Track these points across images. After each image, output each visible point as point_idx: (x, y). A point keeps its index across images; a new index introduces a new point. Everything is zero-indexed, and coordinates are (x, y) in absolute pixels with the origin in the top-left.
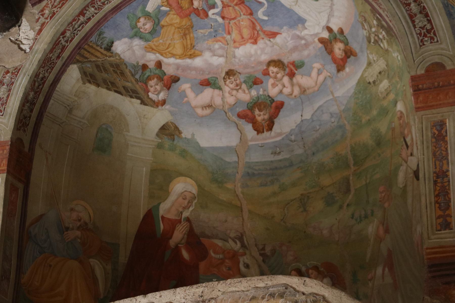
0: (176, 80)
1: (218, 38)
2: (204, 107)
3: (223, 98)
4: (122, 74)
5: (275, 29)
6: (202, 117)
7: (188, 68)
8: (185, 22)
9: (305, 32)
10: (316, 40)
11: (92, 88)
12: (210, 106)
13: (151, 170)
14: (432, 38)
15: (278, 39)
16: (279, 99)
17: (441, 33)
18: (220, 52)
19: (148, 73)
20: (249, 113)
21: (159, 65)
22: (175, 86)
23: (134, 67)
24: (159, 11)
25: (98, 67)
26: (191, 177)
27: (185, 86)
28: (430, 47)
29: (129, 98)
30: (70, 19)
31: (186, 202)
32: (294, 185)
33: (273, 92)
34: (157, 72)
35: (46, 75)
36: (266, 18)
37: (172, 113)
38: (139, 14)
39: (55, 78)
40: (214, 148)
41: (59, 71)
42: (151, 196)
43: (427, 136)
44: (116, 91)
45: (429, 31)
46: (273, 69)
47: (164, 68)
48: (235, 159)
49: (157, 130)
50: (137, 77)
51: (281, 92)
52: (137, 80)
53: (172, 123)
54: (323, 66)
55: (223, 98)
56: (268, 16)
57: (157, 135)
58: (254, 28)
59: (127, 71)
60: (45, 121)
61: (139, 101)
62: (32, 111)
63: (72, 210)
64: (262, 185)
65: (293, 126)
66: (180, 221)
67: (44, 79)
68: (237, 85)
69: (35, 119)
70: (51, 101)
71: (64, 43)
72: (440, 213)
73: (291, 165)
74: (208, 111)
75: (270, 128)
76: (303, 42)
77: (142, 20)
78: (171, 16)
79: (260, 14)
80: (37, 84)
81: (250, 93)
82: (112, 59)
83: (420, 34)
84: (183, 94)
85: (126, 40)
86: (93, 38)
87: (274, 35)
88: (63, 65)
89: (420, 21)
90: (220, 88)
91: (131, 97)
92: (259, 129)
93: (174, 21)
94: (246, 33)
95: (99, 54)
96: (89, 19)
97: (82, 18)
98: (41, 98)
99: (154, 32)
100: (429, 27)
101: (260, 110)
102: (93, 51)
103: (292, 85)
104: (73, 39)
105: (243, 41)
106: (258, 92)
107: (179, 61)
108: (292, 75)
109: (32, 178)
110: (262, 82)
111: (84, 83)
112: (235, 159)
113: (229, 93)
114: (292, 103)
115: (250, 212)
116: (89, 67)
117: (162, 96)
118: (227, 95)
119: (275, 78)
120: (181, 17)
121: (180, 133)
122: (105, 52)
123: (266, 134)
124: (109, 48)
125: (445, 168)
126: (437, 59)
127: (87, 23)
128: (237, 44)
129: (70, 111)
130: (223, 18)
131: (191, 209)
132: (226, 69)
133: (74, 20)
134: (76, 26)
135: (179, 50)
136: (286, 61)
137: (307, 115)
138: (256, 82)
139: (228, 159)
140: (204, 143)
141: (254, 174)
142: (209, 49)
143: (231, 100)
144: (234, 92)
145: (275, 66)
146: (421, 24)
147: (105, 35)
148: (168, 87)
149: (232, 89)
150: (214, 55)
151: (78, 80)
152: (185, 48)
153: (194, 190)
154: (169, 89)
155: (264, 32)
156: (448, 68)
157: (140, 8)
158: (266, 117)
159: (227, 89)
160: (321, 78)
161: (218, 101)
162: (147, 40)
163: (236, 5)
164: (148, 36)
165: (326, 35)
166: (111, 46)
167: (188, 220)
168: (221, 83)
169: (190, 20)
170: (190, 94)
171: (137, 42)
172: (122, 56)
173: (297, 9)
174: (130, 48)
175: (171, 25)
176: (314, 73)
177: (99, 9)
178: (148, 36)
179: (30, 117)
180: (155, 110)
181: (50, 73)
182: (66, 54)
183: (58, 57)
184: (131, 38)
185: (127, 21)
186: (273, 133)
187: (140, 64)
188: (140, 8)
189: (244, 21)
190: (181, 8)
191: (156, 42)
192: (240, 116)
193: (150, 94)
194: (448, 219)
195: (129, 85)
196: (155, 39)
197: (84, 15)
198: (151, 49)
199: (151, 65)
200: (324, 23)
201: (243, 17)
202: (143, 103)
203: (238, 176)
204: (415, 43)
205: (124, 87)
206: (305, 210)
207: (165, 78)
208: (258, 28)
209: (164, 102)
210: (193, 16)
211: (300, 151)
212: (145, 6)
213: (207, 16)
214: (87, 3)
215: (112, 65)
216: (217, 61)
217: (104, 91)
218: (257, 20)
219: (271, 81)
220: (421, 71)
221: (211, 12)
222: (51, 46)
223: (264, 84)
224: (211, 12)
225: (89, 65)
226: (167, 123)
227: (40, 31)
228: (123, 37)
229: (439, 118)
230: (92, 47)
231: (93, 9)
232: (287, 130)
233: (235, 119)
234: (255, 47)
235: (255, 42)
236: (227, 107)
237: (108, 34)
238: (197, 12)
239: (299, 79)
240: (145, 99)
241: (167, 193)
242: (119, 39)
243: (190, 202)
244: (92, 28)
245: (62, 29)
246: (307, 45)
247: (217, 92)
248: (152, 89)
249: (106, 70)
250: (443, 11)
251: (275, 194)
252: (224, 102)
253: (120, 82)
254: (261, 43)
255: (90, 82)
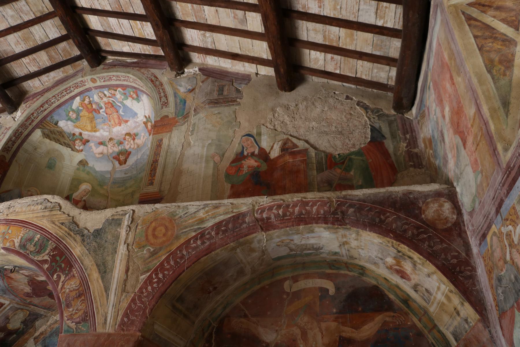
0: (88, 141)
1: (106, 124)
2: (99, 154)
3: (108, 150)
4: (63, 136)
5: (127, 119)
6: (98, 158)
7: (93, 136)
8: (90, 115)
9: (138, 119)
10: (142, 123)
11: (47, 141)
12: (102, 153)
13: (73, 179)
14: (167, 106)
15: (129, 123)
16: (129, 150)
17: (170, 104)
18: (107, 130)
19: (75, 137)
20: (118, 157)
21: (81, 134)
22: (87, 144)
23: (69, 134)
24: (79, 109)
25: (51, 132)
26: (90, 183)
27: (92, 144)
28: (165, 109)
29: (66, 147)
30: (36, 108)
31: (85, 193)
32: (131, 187)
33: (127, 147)
34: (80, 137)
35: (23, 131)
36: (123, 114)
37: (85, 156)
38: (69, 110)
39: (28, 133)
40: (101, 171)
41: (31, 131)
42: (70, 189)
43: (154, 145)
44: (59, 144)
45: (166, 103)
46: (127, 137)
47: (83, 135)
48: (110, 176)
49: (77, 162)
50: (70, 138)
51: (130, 147)
52: (70, 140)
53: (85, 160)
54: (145, 134)
55: (108, 150)
56: (124, 113)
57: (78, 164)
58: (119, 119)
59: (65, 136)
60: (21, 151)
61: (71, 149)
62: (13, 145)
63: (29, 191)
64: (118, 187)
65: (134, 161)
66: (81, 201)
67: (21, 133)
68: (114, 145)
69: (15, 149)
70: (25, 143)
71: (33, 119)
72: (151, 178)
73: (131, 178)
74: (101, 156)
75: (125, 163)
76: (138, 124)
77: (71, 112)
78: (84, 112)
79: (121, 112)
80: (17, 134)
81: (118, 148)
82: (58, 129)
83: (162, 104)
84: (91, 148)
85: (64, 121)
86: (48, 119)
87: (127, 121)
88: (33, 129)
89: (163, 99)
90: (107, 146)
91: (67, 147)
92: (121, 164)
93: (86, 115)
94: (117, 121)
95: (51, 126)
96: (46, 110)
97: (42, 108)
98: (20, 141)
99: (77, 119)
100: (166, 101)
101: (122, 155)
102: (48, 124)
103: (134, 144)
104: (38, 117)
105: (116, 125)
106: (121, 147)
107: (90, 133)
108: (134, 139)
109: (8, 174)
110: (123, 143)
111: (44, 138)
112: (110, 176)
113: (110, 148)
114: (134, 151)
115: (111, 198)
116: (46, 131)
117: (81, 148)
118: (109, 149)
119: (128, 141)
120: (89, 113)
121: (88, 164)
122: (54, 126)
123: (123, 166)
124: (56, 124)
125: (157, 159)
126: (166, 114)
127: (45, 111)
128: (113, 126)
129: (36, 149)
130: (107, 114)
131: (87, 196)
132: (109, 138)
133: (38, 109)
134: (39, 112)
135: (89, 128)
136: (132, 133)
137: (139, 157)
138: (121, 143)
139: (106, 176)
140: (97, 169)
141: (116, 183)
142: (102, 128)
143: (111, 151)
144: (112, 148)
145: (128, 136)
146: (163, 101)
147: (54, 118)
148: (84, 144)
149: (112, 146)
150: (104, 131)
151: (40, 136)
152: (92, 127)
153: (90, 189)
154: (84, 145)
155: (123, 120)
156: (170, 117)
157: (69, 107)
158: (124, 158)
159: (109, 146)
160: (144, 140)
161: (105, 151)
162: (74, 122)
163: (111, 107)
164: (75, 120)
165: (145, 120)
166: (57, 123)
167: (85, 201)
168: (107, 143)
169: (93, 114)
170: (94, 148)
171: (69, 122)
172: (63, 128)
173: (133, 108)
174: (67, 125)
175: (85, 116)
176: (142, 138)
177: (50, 105)
178: (75, 120)
179: (12, 148)
180: (78, 153)
181: (25, 131)
182: (34, 124)
183: (30, 124)
184: (67, 120)
185: (64, 112)
186: (126, 165)
187: (72, 133)
188: (69, 107)
189: (115, 115)
190: (88, 108)
191: (77, 124)
192: (114, 158)
193: (76, 147)
194: (153, 181)
195: (66, 141)
196: (78, 122)
197: (43, 107)
198: (77, 127)
199: (77, 134)
200: (143, 115)
201: (114, 113)
202: (72, 150)
203: (110, 183)
204: (159, 108)
205: (64, 142)
206: (133, 197)
207: (83, 140)
208: (121, 119)
209: (82, 151)
210: (94, 112)
211: (135, 172)
212: (71, 106)
213: (100, 113)
214: (44, 102)
215: (58, 132)
216: (106, 134)
217: (54, 143)
218: (120, 114)
219: (127, 142)
220: (159, 119)
221: (101, 111)
222: (26, 119)
223: (124, 144)
224: (101, 111)
225: (46, 130)
226: (83, 160)
227: (23, 113)
228: (63, 119)
229: (161, 137)
230: (48, 122)
231: (47, 105)
232: (131, 164)
233: (112, 159)
234: (120, 127)
235: (120, 125)
236: (109, 154)
237: (56, 118)
238: (94, 110)
239: (136, 141)
240: (73, 148)
241: (78, 189)
242: (61, 120)
243: (87, 193)
244: (47, 114)
245: (32, 112)
246: (139, 126)
247: (105, 147)
248: (77, 144)
249: (55, 133)
250: (173, 95)
251: (122, 191)
252: (108, 152)
253: (62, 140)
254: (123, 126)
255: (46, 138)
